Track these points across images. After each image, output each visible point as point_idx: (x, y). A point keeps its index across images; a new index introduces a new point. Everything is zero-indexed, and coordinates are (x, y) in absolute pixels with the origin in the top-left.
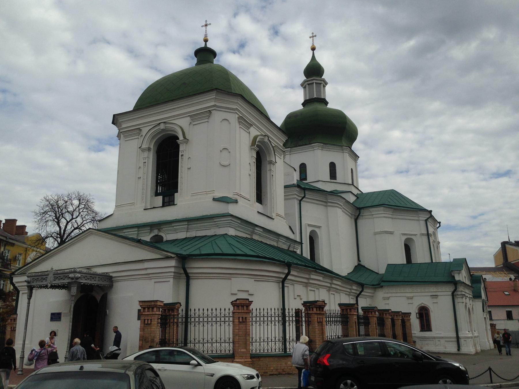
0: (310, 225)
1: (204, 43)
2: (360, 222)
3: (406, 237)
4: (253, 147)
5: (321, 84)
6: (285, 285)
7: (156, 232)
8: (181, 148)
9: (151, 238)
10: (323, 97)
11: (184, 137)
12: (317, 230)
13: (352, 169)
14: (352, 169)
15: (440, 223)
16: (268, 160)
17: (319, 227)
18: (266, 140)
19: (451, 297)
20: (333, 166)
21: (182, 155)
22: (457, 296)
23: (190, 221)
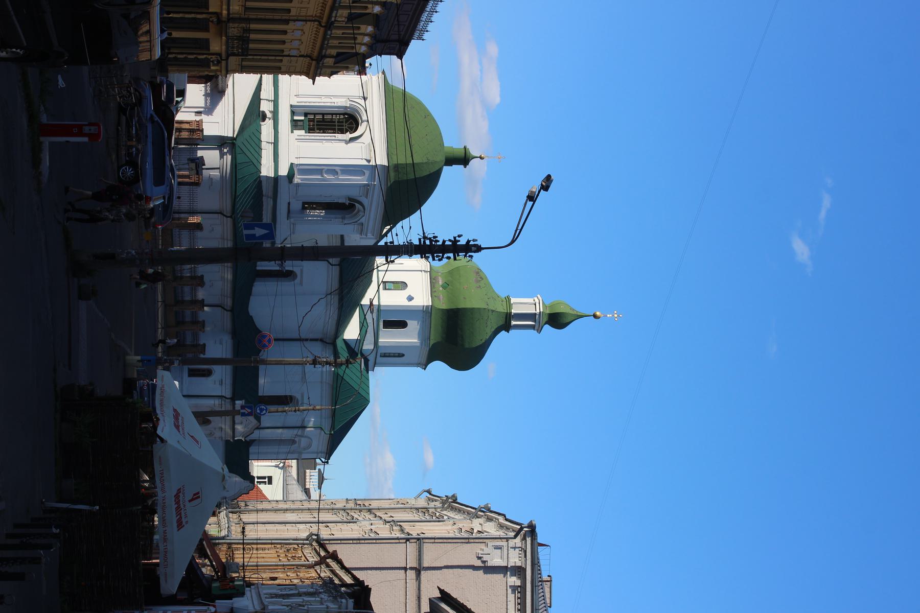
0: (302, 271)
1: (479, 156)
2: (319, 344)
3: (298, 396)
4: (347, 199)
5: (535, 321)
6: (220, 215)
7: (269, 115)
8: (340, 136)
9: (263, 112)
10: (513, 323)
11: (352, 140)
12: (297, 281)
13: (403, 355)
14: (403, 355)
15: (327, 462)
16: (346, 216)
17: (301, 284)
18: (361, 213)
19: (220, 395)
20: (402, 324)
21: (335, 136)
22: (220, 400)
23: (276, 144)
